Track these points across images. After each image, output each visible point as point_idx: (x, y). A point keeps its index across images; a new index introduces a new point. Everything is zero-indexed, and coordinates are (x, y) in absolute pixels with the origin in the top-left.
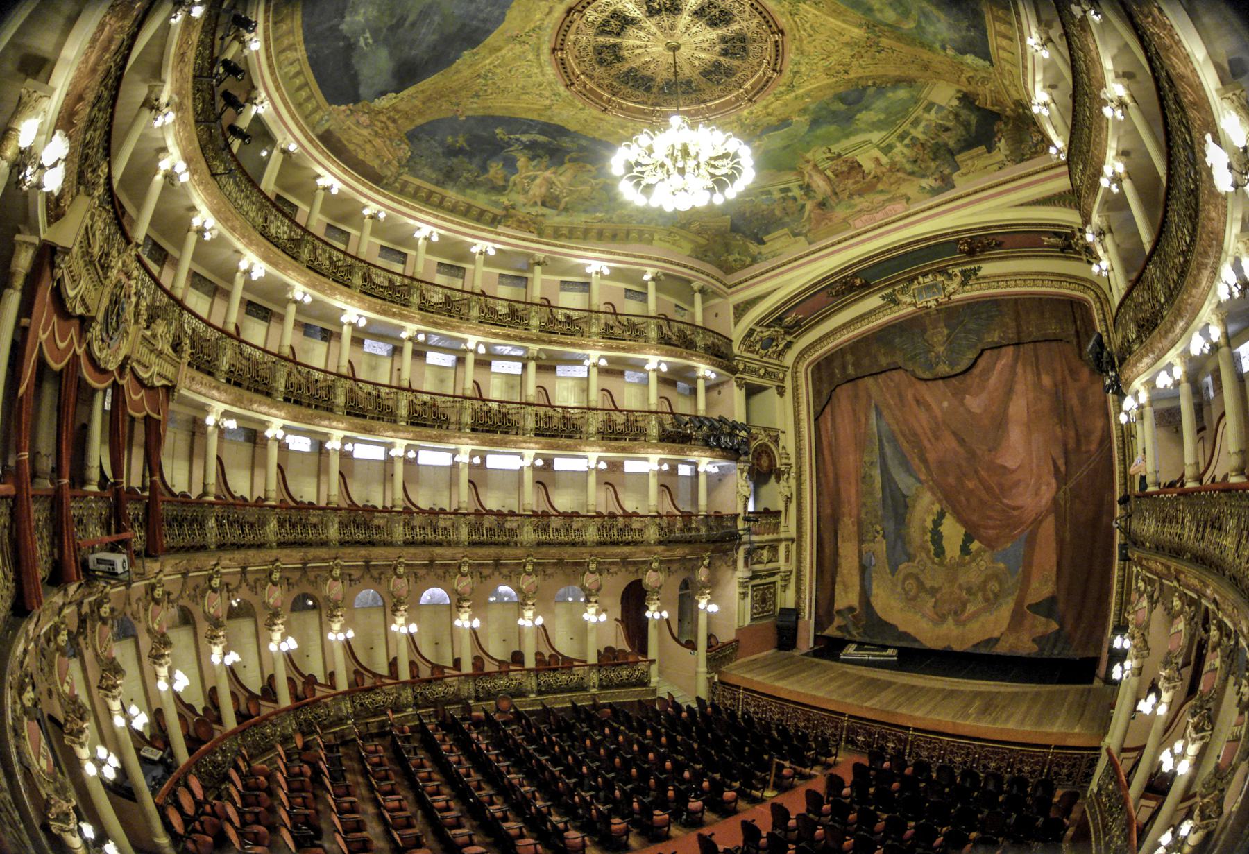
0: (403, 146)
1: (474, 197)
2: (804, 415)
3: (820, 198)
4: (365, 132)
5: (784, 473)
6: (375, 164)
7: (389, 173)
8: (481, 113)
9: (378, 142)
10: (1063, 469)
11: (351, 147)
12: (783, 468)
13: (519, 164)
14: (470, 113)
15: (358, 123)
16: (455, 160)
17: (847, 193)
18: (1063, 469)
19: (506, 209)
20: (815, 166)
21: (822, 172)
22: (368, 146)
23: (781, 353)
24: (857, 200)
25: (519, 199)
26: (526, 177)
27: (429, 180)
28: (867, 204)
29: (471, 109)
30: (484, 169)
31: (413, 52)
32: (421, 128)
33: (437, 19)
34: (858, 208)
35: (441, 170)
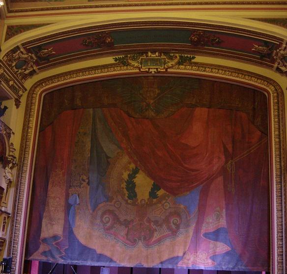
2: (33, 124)
5: (9, 162)
10: (230, 150)
12: (10, 158)
18: (230, 150)
23: (25, 77)
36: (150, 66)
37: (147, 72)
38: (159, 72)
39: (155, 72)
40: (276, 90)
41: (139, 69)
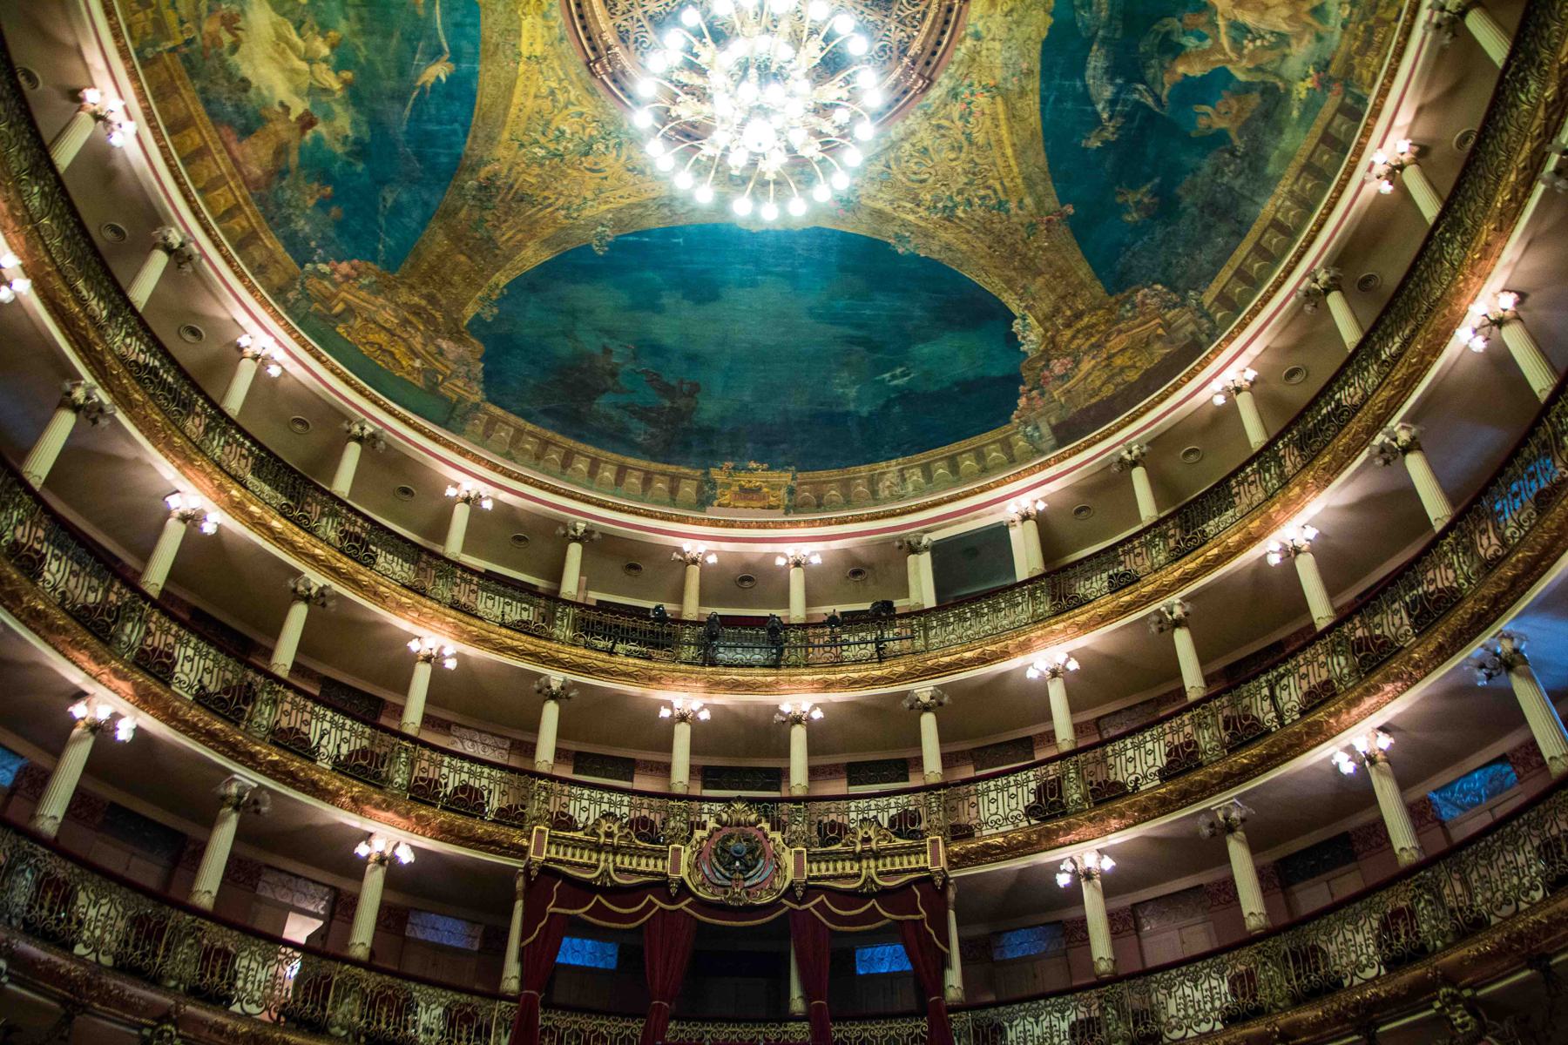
0: (1139, 296)
1: (1287, 158)
4: (1086, 366)
6: (1160, 351)
7: (1191, 327)
8: (1047, 189)
9: (1115, 343)
11: (1108, 391)
13: (1197, 70)
14: (1051, 203)
15: (1064, 378)
16: (1188, 200)
19: (1325, 84)
22: (1118, 361)
25: (1301, 52)
26: (1237, 45)
27: (1229, 251)
29: (1039, 203)
30: (1218, 139)
31: (918, 313)
32: (1098, 270)
33: (840, 304)
35: (1208, 227)
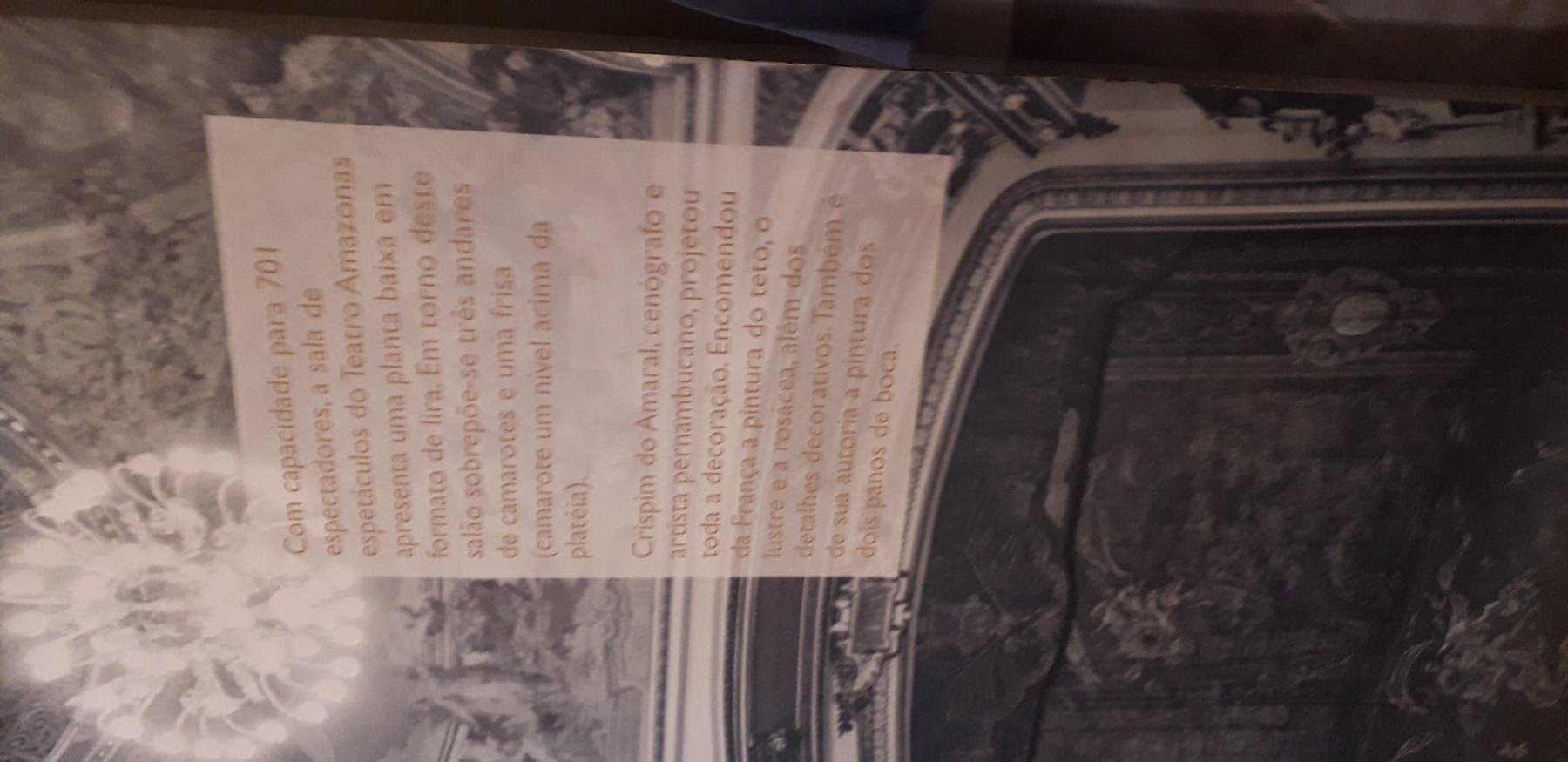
3: (527, 716)
17: (547, 654)
20: (437, 671)
21: (460, 672)
24: (576, 643)
28: (598, 629)
34: (599, 653)
36: (882, 623)
37: (904, 633)
38: (909, 598)
39: (906, 610)
40: (1030, 197)
41: (888, 658)
